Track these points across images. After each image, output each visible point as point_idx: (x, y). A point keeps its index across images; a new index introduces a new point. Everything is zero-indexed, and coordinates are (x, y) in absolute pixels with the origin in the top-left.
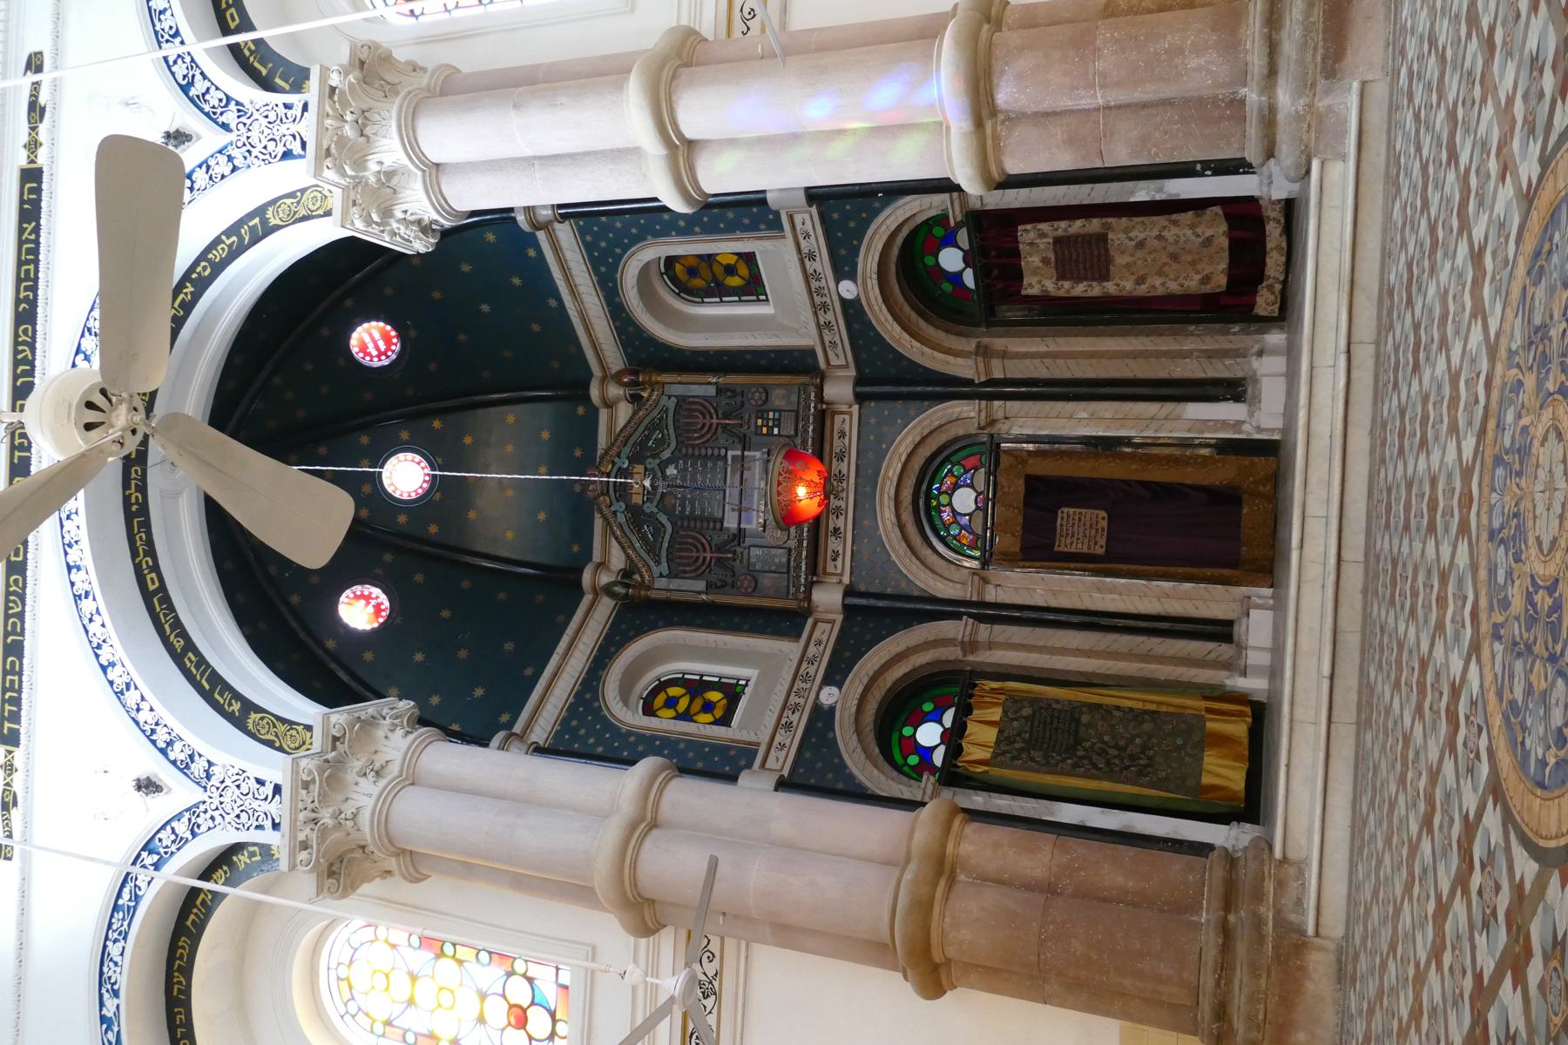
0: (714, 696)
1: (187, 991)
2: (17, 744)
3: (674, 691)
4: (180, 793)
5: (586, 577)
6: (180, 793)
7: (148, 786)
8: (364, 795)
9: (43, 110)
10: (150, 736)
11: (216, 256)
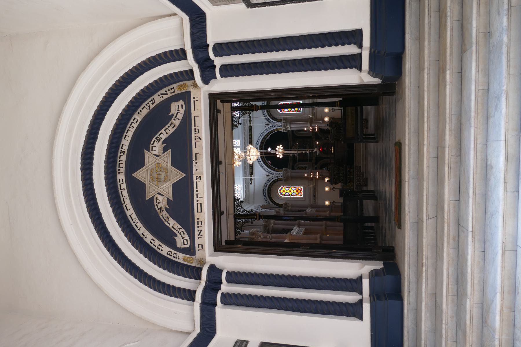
0: (304, 168)
1: (270, 193)
2: (252, 174)
3: (300, 168)
4: (271, 176)
5: (289, 158)
6: (271, 176)
7: (268, 176)
8: (289, 174)
9: (251, 121)
10: (268, 172)
11: (269, 133)
